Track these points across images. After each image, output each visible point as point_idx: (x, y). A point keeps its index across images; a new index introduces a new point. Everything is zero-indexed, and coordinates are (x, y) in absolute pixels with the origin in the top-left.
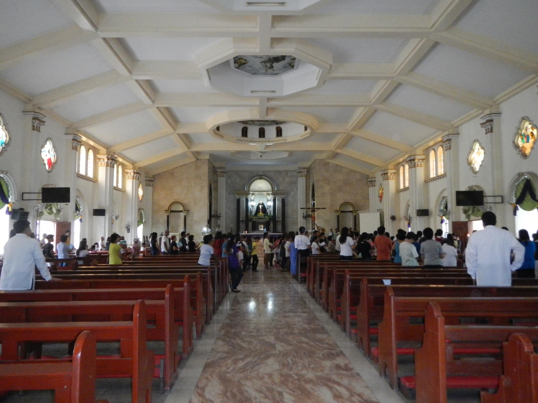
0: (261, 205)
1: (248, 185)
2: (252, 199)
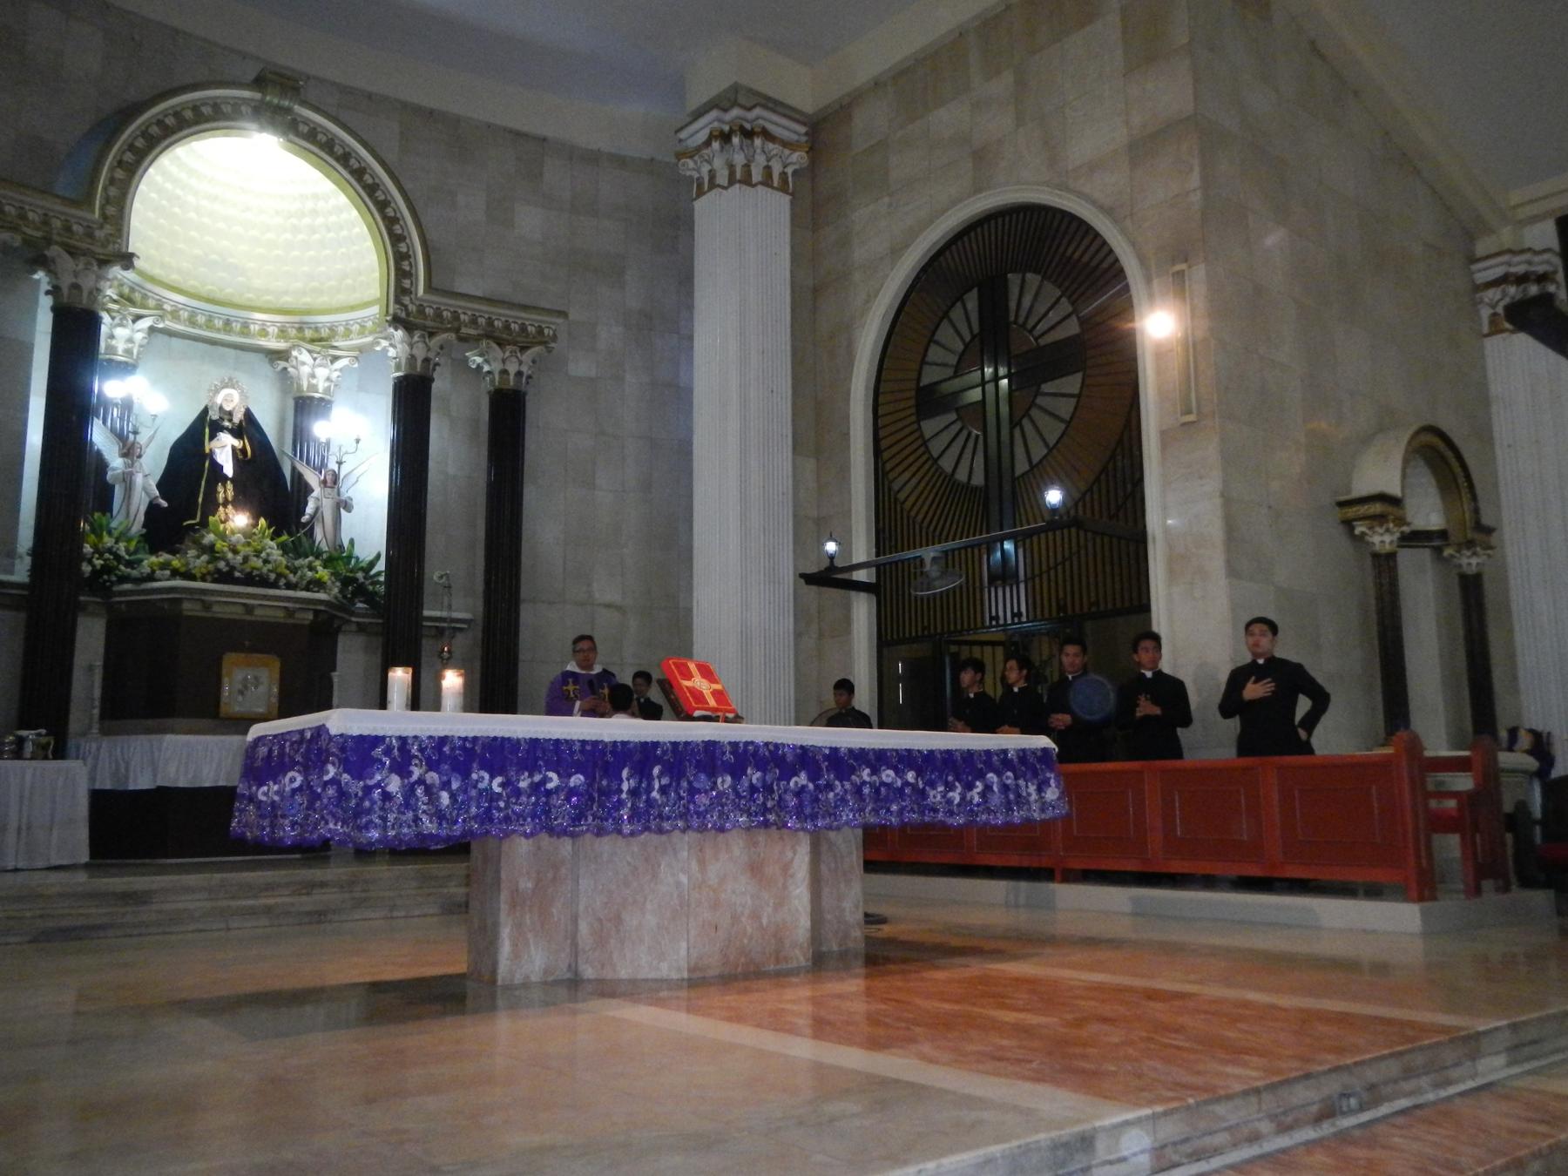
0: (237, 432)
1: (109, 144)
2: (121, 346)
